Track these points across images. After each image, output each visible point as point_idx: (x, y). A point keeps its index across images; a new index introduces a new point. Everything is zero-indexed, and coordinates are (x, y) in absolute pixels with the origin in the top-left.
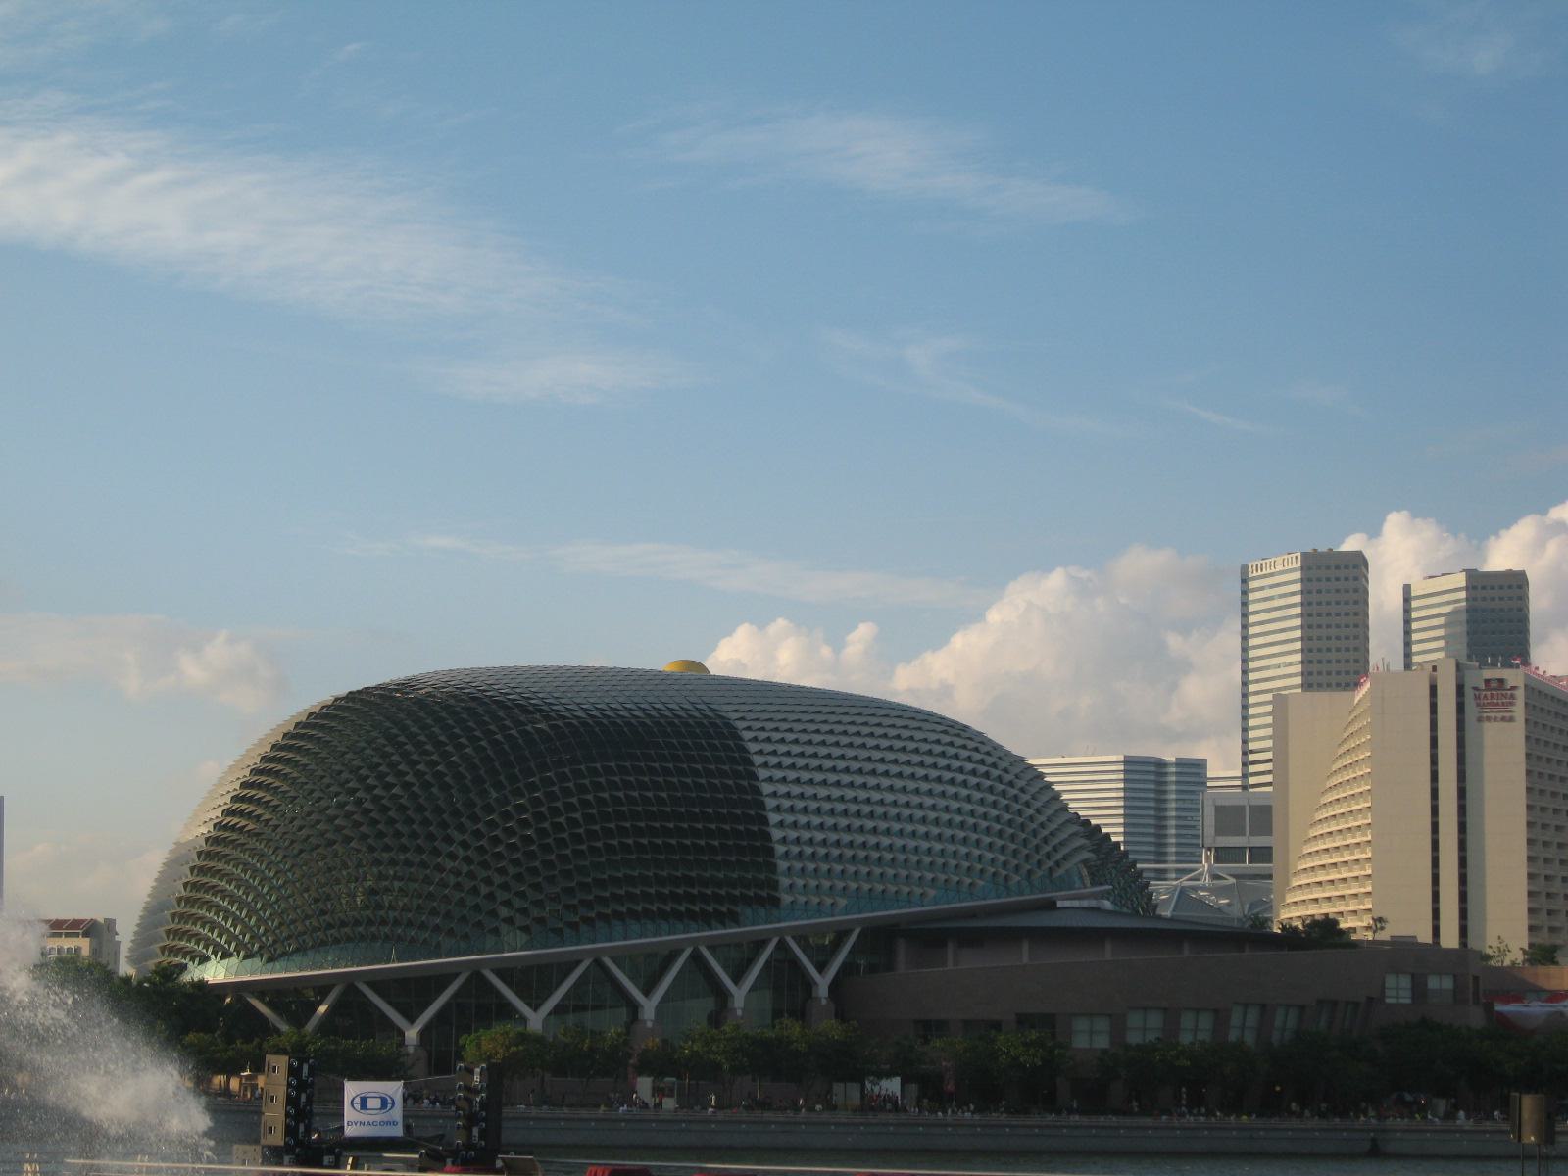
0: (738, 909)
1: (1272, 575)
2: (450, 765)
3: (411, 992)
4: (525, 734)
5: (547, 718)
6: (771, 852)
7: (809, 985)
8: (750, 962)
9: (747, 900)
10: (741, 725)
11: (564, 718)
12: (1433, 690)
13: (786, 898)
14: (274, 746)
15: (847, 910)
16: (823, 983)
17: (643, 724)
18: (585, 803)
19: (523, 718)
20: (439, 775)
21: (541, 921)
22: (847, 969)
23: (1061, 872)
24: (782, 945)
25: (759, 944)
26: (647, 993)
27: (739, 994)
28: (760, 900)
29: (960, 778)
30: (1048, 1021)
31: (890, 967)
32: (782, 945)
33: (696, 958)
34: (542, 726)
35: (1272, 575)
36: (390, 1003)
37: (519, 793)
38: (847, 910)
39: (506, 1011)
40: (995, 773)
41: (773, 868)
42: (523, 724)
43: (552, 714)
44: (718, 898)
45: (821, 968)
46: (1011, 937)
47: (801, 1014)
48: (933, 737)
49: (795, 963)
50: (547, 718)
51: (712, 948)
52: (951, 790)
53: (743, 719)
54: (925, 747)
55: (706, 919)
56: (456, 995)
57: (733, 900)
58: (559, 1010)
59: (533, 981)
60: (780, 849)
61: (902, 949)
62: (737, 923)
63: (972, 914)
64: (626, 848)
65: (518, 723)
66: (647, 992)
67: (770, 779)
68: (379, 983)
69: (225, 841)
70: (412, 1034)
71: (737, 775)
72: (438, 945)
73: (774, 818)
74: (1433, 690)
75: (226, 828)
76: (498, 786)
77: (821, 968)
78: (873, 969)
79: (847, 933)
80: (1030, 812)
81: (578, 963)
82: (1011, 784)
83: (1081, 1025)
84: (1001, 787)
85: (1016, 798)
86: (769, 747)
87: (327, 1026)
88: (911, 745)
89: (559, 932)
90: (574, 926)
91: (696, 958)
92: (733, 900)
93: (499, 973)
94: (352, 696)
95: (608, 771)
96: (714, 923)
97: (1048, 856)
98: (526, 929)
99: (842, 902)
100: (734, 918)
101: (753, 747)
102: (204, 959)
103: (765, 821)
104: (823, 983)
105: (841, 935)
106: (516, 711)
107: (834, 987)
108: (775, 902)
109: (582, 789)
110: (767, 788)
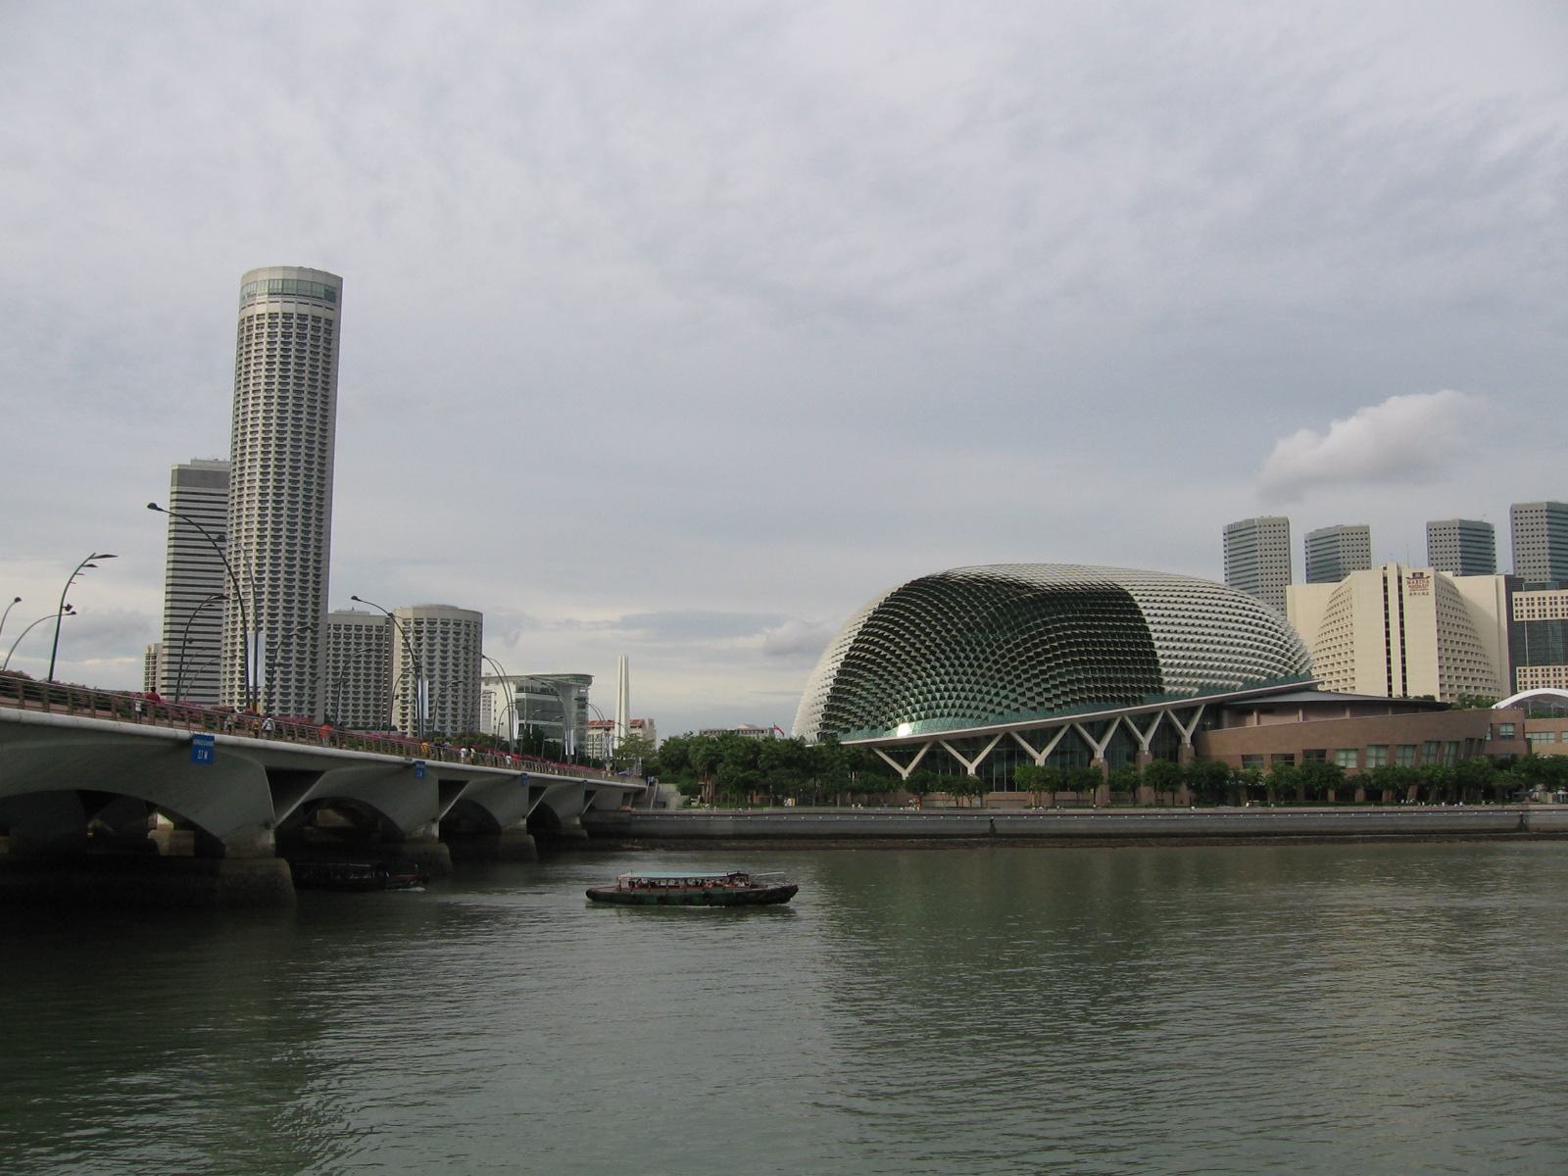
2: (983, 618)
3: (970, 745)
4: (1021, 600)
7: (1179, 738)
9: (1147, 690)
10: (1132, 593)
12: (1385, 580)
13: (1168, 689)
16: (1187, 735)
20: (977, 624)
22: (1201, 727)
23: (1304, 671)
24: (1166, 716)
27: (1145, 742)
28: (1154, 690)
30: (1322, 753)
31: (1218, 725)
32: (1166, 716)
33: (1123, 725)
37: (1022, 632)
39: (1024, 754)
42: (1019, 594)
44: (1133, 689)
47: (1174, 755)
55: (1127, 702)
56: (995, 747)
57: (1140, 689)
58: (1053, 753)
59: (1038, 737)
61: (1226, 717)
62: (1142, 704)
66: (1098, 742)
67: (1152, 623)
68: (953, 741)
69: (853, 665)
70: (971, 769)
72: (987, 718)
74: (1385, 580)
75: (853, 657)
81: (1062, 727)
83: (1342, 755)
91: (1123, 725)
92: (1140, 689)
93: (1022, 734)
98: (1034, 709)
102: (847, 731)
104: (1187, 735)
110: (1152, 628)
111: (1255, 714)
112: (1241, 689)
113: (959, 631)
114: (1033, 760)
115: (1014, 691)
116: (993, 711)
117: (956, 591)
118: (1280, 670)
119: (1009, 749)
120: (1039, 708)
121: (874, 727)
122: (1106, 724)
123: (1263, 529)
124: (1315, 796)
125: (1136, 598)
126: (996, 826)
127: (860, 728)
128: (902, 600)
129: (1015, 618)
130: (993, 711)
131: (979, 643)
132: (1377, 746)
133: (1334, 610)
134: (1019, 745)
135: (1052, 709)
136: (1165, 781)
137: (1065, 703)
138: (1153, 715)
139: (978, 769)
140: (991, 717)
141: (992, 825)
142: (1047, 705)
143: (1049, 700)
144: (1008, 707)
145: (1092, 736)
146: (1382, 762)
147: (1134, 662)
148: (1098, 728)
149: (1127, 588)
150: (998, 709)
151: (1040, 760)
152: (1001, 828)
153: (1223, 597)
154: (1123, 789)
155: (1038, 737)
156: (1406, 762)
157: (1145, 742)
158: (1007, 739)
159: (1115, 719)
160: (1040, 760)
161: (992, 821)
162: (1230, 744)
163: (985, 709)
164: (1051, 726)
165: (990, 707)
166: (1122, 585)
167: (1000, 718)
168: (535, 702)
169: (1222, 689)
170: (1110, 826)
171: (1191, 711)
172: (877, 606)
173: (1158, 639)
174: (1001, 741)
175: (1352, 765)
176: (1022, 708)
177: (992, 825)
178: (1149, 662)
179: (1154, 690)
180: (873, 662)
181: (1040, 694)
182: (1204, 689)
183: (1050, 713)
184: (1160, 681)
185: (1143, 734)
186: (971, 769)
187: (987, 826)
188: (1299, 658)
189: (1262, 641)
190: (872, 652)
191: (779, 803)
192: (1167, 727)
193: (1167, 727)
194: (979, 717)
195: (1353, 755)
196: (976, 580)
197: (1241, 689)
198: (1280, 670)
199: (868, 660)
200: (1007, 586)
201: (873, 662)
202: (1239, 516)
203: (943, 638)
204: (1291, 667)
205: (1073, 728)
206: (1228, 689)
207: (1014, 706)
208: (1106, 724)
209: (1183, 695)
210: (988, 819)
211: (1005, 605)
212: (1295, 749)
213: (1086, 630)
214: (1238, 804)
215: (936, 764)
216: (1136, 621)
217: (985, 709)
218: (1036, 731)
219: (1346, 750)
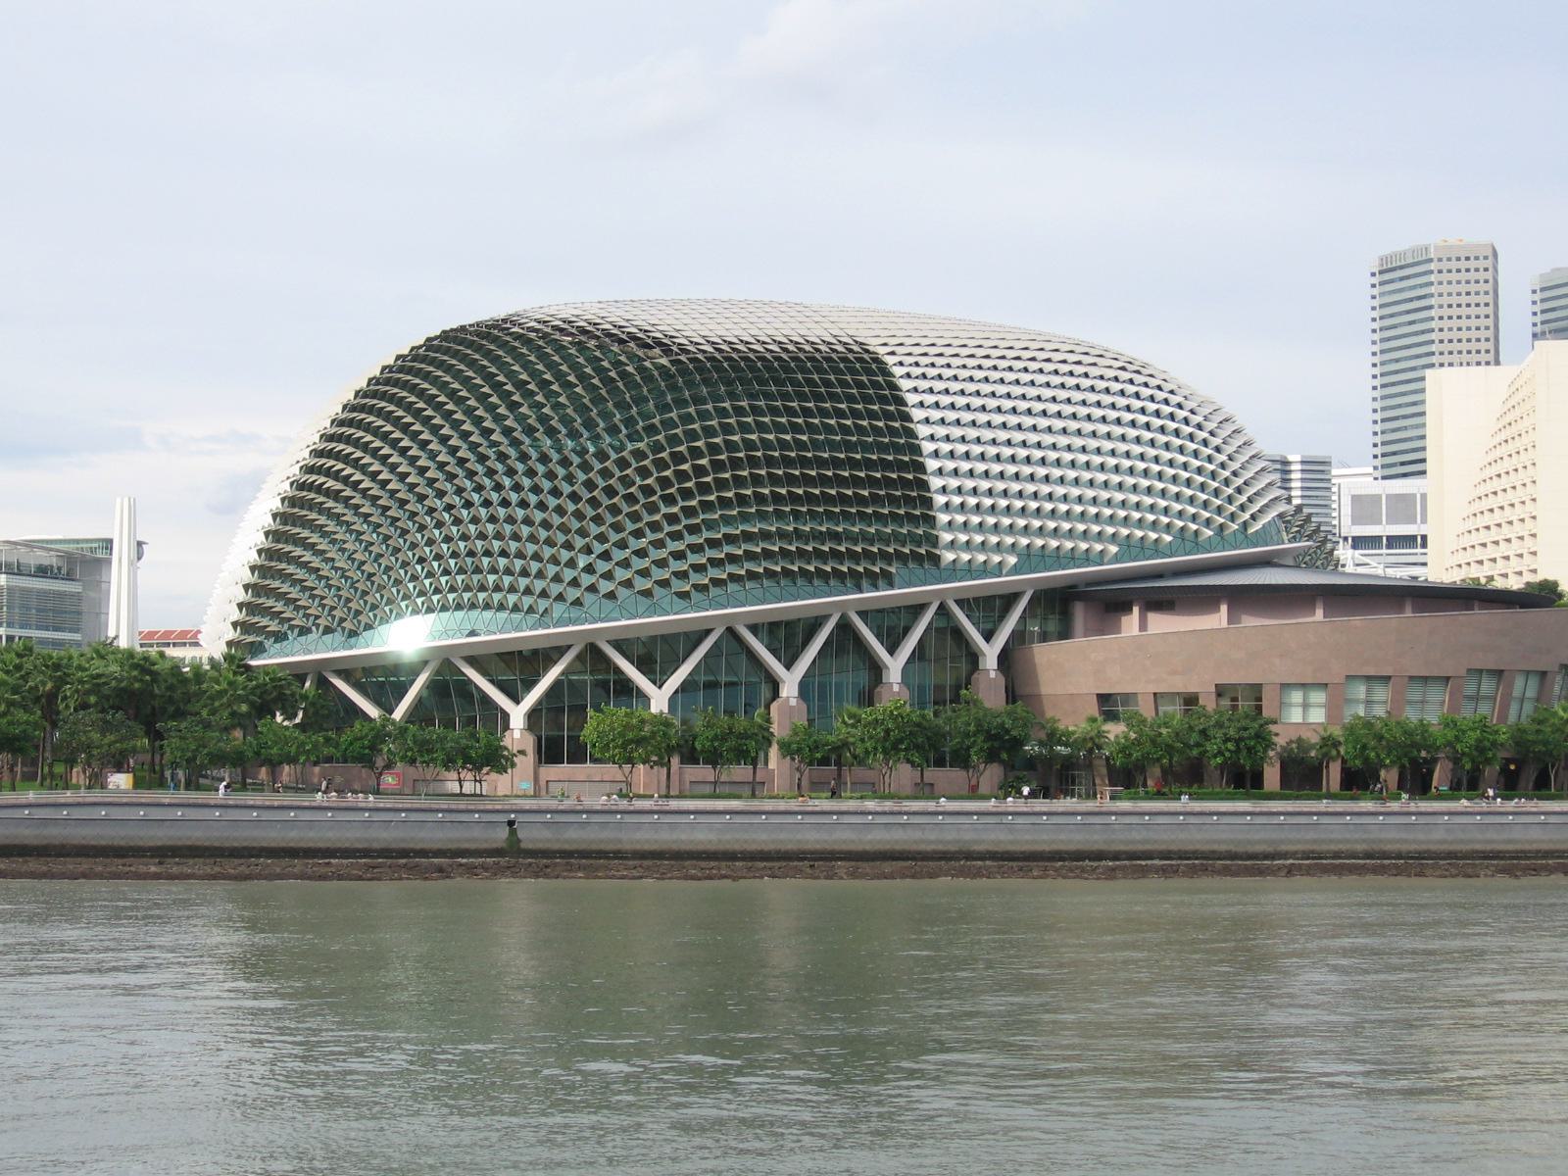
0: (893, 570)
1: (1401, 267)
5: (667, 351)
6: (928, 503)
7: (974, 658)
8: (906, 630)
9: (900, 557)
10: (890, 360)
11: (688, 352)
13: (949, 556)
14: (357, 394)
15: (1015, 570)
17: (779, 359)
18: (714, 449)
19: (640, 353)
21: (664, 583)
22: (1019, 637)
24: (943, 609)
25: (917, 610)
26: (788, 666)
27: (894, 666)
28: (917, 557)
29: (1142, 419)
30: (1256, 691)
32: (943, 609)
33: (845, 628)
34: (664, 361)
35: (1401, 267)
36: (492, 681)
38: (1015, 570)
39: (626, 689)
40: (1181, 414)
41: (931, 521)
42: (641, 360)
43: (675, 348)
45: (988, 636)
46: (1203, 600)
48: (1111, 373)
49: (958, 634)
50: (667, 351)
51: (863, 615)
52: (1132, 433)
53: (893, 353)
54: (1101, 385)
55: (856, 580)
57: (886, 557)
58: (685, 687)
59: (656, 655)
60: (940, 500)
61: (1079, 614)
62: (891, 585)
63: (1158, 574)
64: (760, 499)
65: (631, 356)
66: (788, 666)
70: (517, 715)
71: (888, 416)
73: (932, 465)
76: (613, 430)
77: (988, 636)
78: (1044, 637)
79: (1014, 597)
80: (1222, 458)
81: (708, 632)
82: (1199, 427)
83: (1297, 697)
84: (1188, 430)
85: (1205, 443)
86: (924, 385)
87: (417, 713)
88: (1086, 383)
89: (684, 595)
90: (701, 589)
91: (845, 628)
92: (886, 557)
93: (619, 645)
94: (445, 335)
95: (739, 411)
96: (865, 583)
97: (1242, 508)
99: (1012, 560)
100: (889, 580)
101: (905, 384)
102: (279, 637)
103: (921, 468)
104: (990, 654)
105: (1009, 600)
106: (632, 344)
107: (1004, 658)
108: (935, 560)
109: (709, 432)
110: (923, 431)
111: (1136, 610)
112: (1117, 559)
113: (507, 432)
114: (645, 699)
115: (625, 564)
116: (560, 597)
117: (512, 351)
118: (1208, 522)
119: (597, 679)
120: (658, 591)
121: (328, 630)
122: (814, 625)
123: (1445, 266)
124: (1245, 780)
125: (898, 371)
126: (521, 835)
127: (304, 631)
128: (417, 373)
129: (664, 408)
130: (560, 597)
131: (544, 459)
132: (1369, 678)
133: (1507, 420)
134: (618, 670)
135: (684, 595)
136: (932, 746)
137: (717, 582)
138: (917, 610)
139: (533, 716)
140: (558, 609)
141: (513, 832)
142: (678, 585)
143: (682, 575)
144: (592, 589)
145: (774, 652)
146: (1380, 711)
147: (875, 499)
148: (788, 637)
149: (882, 350)
150: (573, 594)
151: (659, 699)
152: (531, 836)
153: (1094, 371)
154: (825, 761)
155: (656, 655)
156: (1429, 711)
157: (894, 666)
158: (592, 655)
159: (827, 617)
160: (659, 699)
161: (511, 823)
162: (1079, 675)
163: (544, 594)
164: (644, 634)
165: (555, 589)
166: (874, 345)
167: (575, 612)
168: (26, 592)
169: (1073, 558)
170: (764, 836)
171: (1009, 600)
172: (364, 384)
173: (936, 454)
174: (579, 657)
175: (1317, 716)
176: (622, 593)
177: (513, 832)
178: (909, 501)
179: (917, 557)
180: (335, 495)
181: (661, 564)
182: (1029, 558)
183: (680, 603)
184: (934, 541)
185: (892, 651)
186: (517, 715)
187: (503, 833)
188: (1250, 500)
189: (1171, 463)
190: (336, 476)
191: (97, 781)
192: (947, 632)
193: (947, 632)
194: (531, 610)
195: (1318, 697)
196: (561, 330)
197: (1117, 559)
198: (1208, 522)
199: (328, 493)
200: (621, 342)
201: (335, 495)
202: (1402, 240)
203: (473, 447)
204: (1233, 517)
205: (731, 631)
206: (1087, 557)
207: (605, 587)
208: (814, 625)
209: (985, 570)
210: (504, 818)
211: (608, 382)
212: (1202, 683)
213: (794, 440)
214: (1092, 795)
215: (451, 714)
216: (888, 416)
217: (544, 594)
218: (654, 639)
219: (1303, 686)
